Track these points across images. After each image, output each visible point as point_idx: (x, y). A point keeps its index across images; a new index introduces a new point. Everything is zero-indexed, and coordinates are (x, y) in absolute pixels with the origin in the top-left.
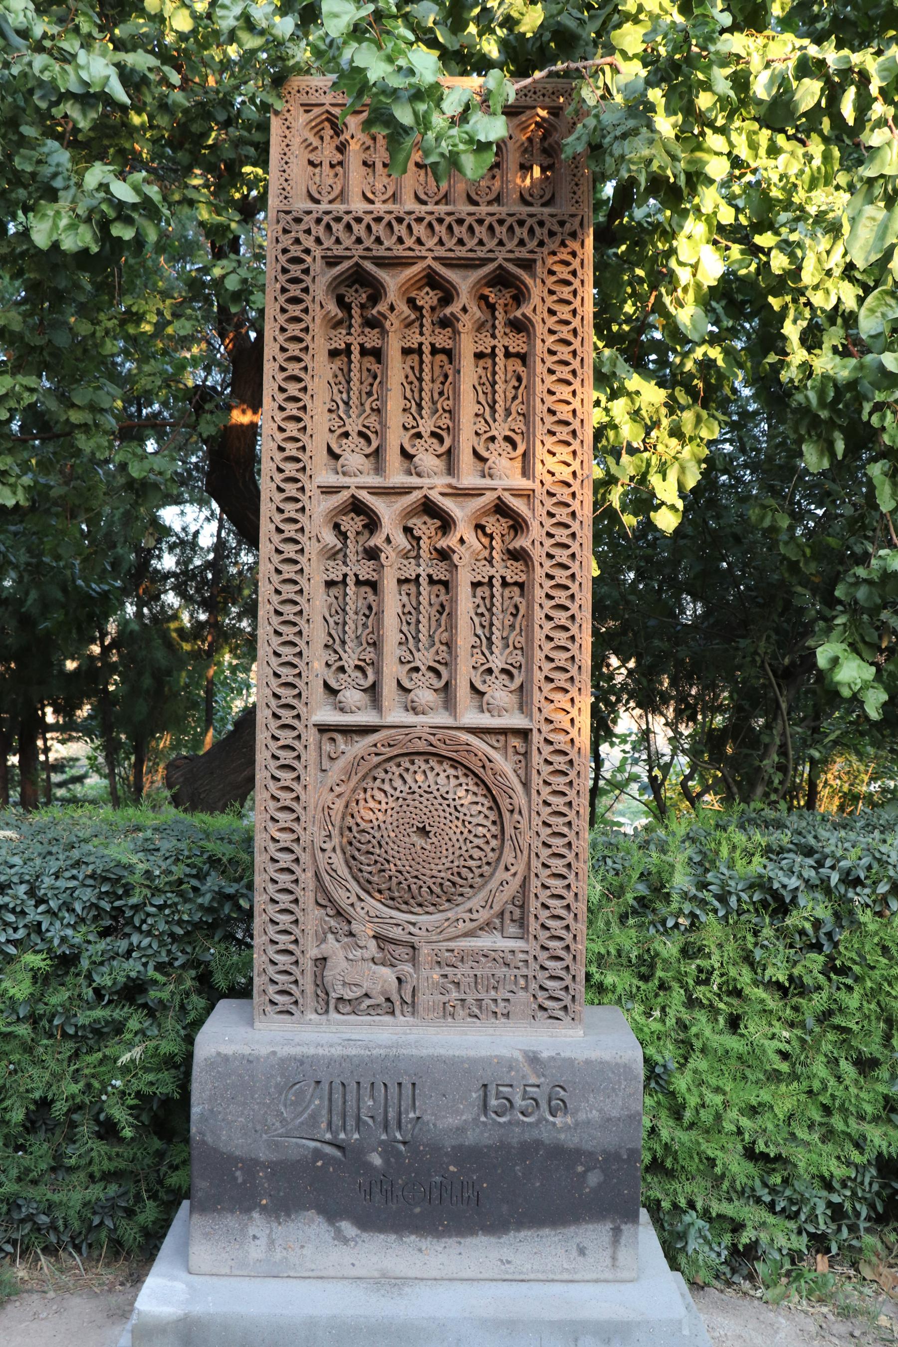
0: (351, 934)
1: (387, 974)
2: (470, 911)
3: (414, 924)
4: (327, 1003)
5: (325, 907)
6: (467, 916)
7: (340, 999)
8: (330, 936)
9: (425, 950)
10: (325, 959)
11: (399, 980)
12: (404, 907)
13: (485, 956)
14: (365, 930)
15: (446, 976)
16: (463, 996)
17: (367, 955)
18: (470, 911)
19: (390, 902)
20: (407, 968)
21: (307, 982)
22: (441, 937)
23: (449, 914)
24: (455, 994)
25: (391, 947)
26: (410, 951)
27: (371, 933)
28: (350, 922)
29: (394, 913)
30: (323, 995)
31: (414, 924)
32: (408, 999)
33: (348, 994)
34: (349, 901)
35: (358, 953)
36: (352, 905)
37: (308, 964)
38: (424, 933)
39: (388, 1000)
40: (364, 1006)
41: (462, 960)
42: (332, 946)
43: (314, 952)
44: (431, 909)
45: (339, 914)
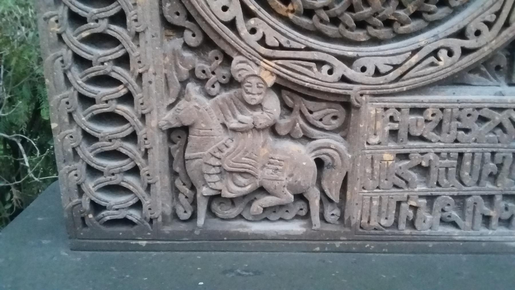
0: (232, 83)
1: (301, 154)
2: (461, 34)
3: (349, 61)
4: (194, 203)
5: (179, 30)
6: (456, 44)
7: (216, 198)
8: (192, 87)
9: (371, 109)
10: (185, 129)
11: (320, 163)
12: (330, 30)
13: (482, 119)
14: (257, 74)
15: (405, 156)
16: (435, 191)
17: (263, 118)
18: (461, 34)
19: (305, 21)
20: (335, 141)
21: (156, 165)
22: (404, 84)
23: (421, 39)
24: (421, 188)
25: (306, 105)
26: (340, 111)
27: (271, 81)
28: (228, 60)
29: (312, 42)
30: (186, 190)
31: (349, 61)
32: (334, 195)
33: (232, 189)
34: (227, 16)
35: (247, 118)
36: (232, 25)
37: (152, 134)
38: (366, 78)
39: (300, 197)
40: (257, 207)
41: (439, 128)
42: (197, 104)
43: (163, 118)
44: (383, 32)
45: (208, 43)
